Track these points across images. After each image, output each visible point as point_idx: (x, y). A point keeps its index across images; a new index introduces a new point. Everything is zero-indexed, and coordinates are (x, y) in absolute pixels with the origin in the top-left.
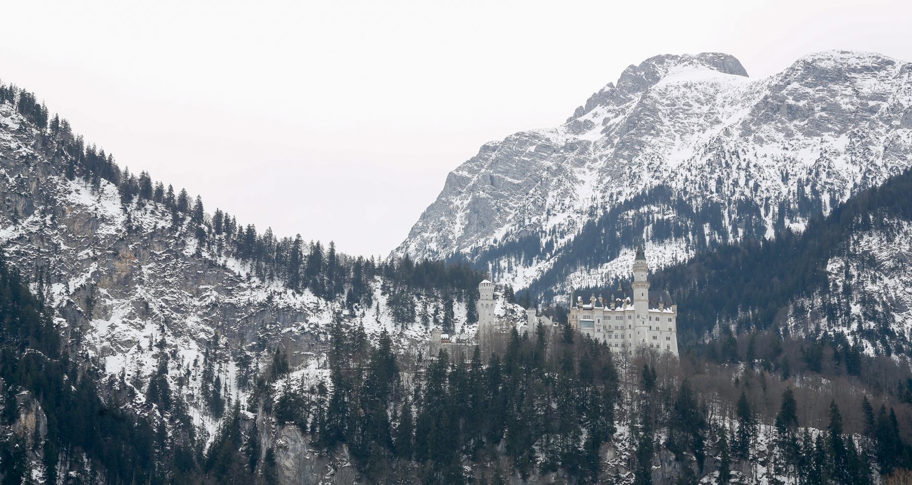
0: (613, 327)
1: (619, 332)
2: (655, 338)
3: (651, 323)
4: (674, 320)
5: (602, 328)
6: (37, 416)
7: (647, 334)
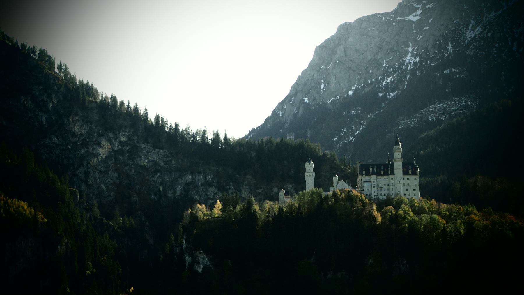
1: (386, 187)
2: (407, 190)
3: (404, 182)
4: (418, 179)
7: (402, 188)
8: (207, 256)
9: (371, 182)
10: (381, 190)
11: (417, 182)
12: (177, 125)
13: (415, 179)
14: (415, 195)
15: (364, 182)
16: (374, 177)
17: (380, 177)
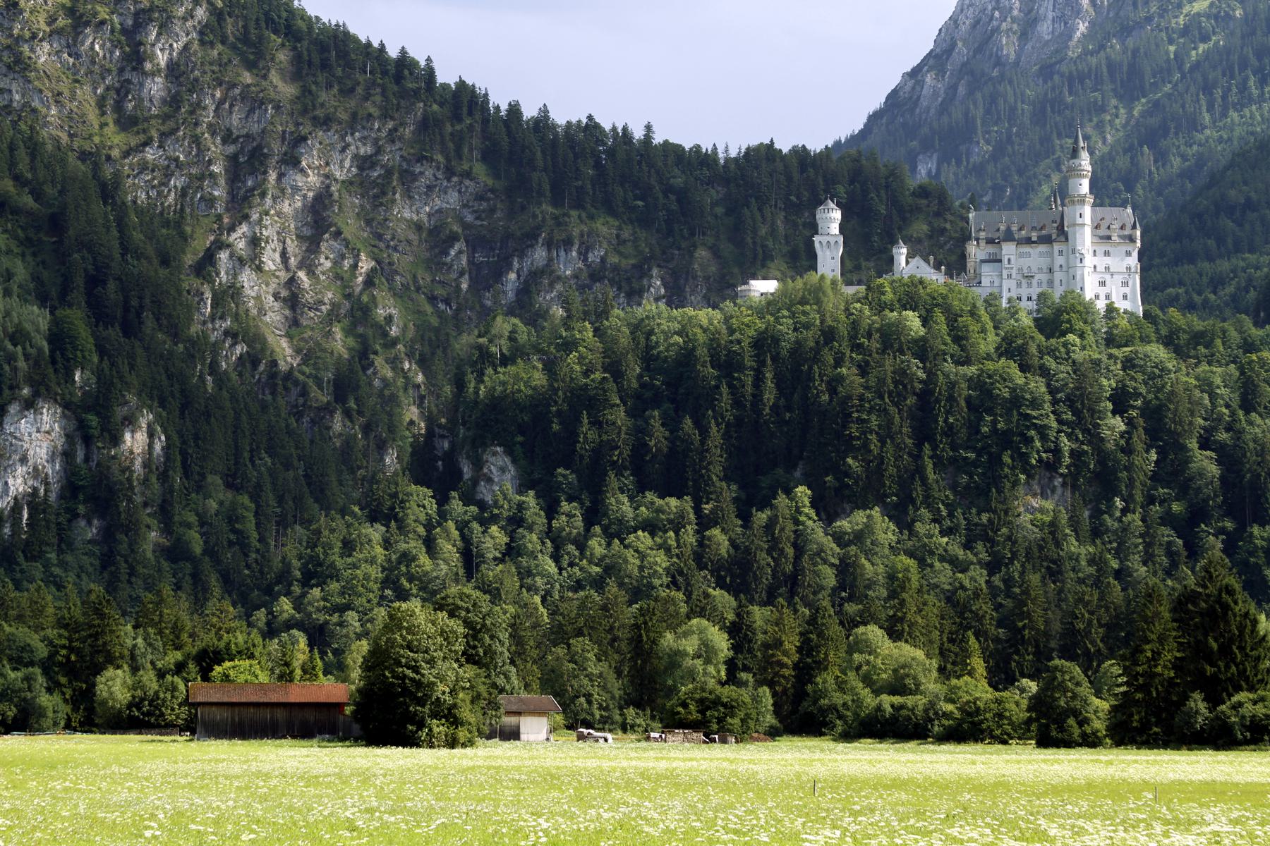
0: (1034, 269)
2: (1103, 284)
4: (1135, 254)
5: (1014, 272)
6: (151, 435)
8: (514, 461)
9: (1000, 261)
10: (1030, 285)
11: (1133, 261)
12: (514, 109)
13: (1129, 254)
14: (1125, 297)
15: (983, 261)
16: (1008, 249)
17: (1026, 249)
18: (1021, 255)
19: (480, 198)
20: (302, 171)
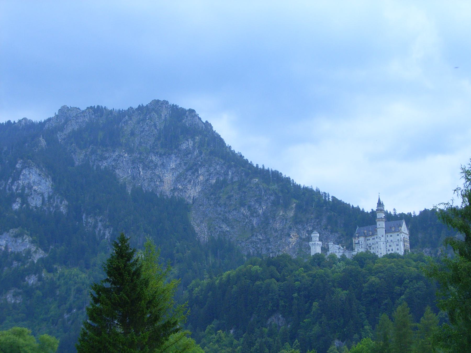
0: (371, 244)
2: (390, 246)
13: (398, 235)
18: (368, 240)
19: (340, 238)
20: (291, 237)
